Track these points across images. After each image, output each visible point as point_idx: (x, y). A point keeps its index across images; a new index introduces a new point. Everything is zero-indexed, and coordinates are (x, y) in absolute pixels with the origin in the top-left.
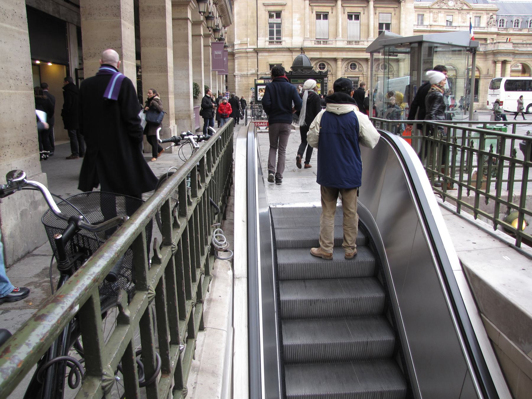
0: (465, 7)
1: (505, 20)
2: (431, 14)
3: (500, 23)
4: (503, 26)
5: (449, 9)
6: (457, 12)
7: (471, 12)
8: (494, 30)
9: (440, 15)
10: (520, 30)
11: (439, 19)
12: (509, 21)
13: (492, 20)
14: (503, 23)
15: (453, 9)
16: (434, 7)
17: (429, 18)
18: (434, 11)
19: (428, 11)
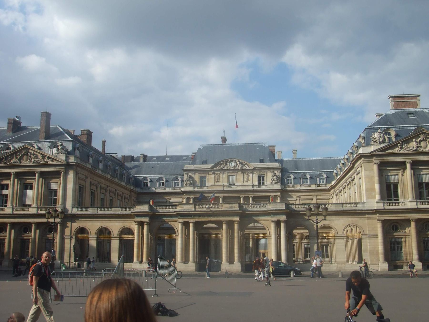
0: (246, 167)
1: (292, 177)
2: (213, 176)
4: (291, 183)
5: (230, 170)
9: (221, 175)
10: (309, 186)
11: (221, 179)
13: (275, 178)
15: (234, 170)
16: (215, 169)
17: (211, 179)
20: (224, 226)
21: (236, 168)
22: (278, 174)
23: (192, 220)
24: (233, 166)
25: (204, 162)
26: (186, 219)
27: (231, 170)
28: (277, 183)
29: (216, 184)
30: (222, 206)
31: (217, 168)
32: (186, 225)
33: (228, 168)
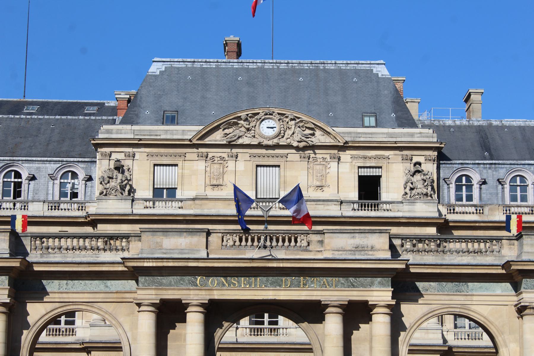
0: (319, 138)
2: (201, 165)
3: (459, 188)
4: (470, 198)
5: (260, 146)
6: (293, 155)
7: (346, 156)
8: (425, 209)
9: (231, 164)
12: (492, 182)
13: (418, 177)
14: (469, 187)
15: (277, 146)
16: (207, 141)
18: (212, 152)
19: (192, 153)
20: (333, 324)
21: (283, 142)
22: (430, 168)
23: (195, 294)
24: (271, 133)
25: (171, 119)
26: (171, 294)
27: (268, 147)
28: (426, 195)
29: (211, 193)
30: (321, 242)
31: (217, 137)
32: (169, 315)
33: (255, 142)
